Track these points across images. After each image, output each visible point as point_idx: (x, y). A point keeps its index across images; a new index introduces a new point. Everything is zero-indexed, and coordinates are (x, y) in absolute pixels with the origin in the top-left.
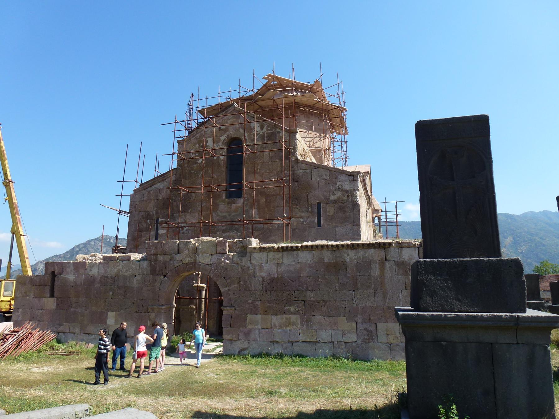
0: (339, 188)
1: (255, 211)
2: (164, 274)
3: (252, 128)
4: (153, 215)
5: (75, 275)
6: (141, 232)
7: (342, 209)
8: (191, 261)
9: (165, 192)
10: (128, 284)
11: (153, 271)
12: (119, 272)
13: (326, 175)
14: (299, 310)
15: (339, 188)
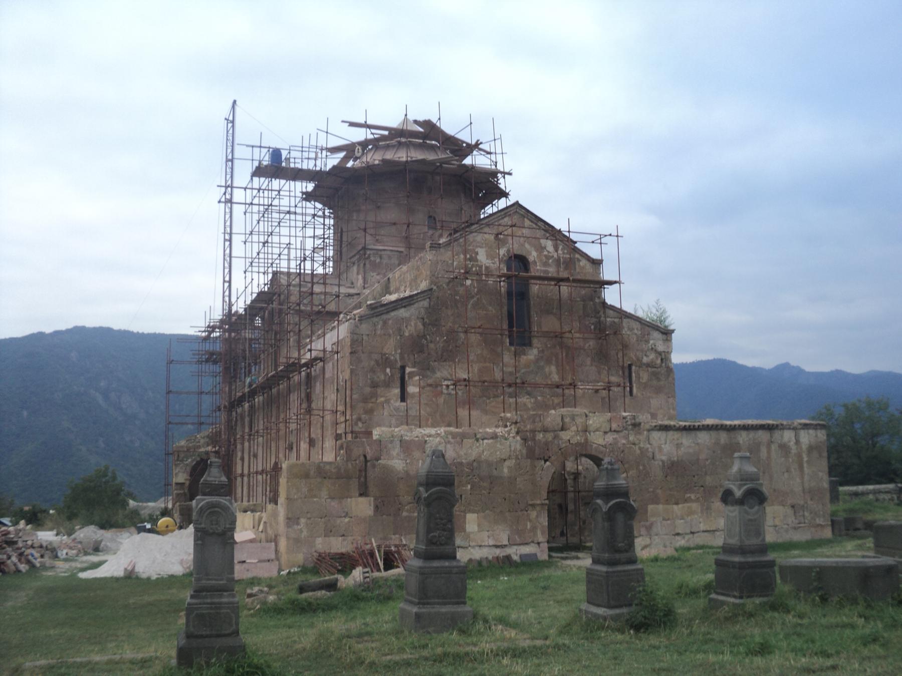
0: (652, 348)
1: (553, 368)
2: (546, 458)
3: (543, 246)
4: (396, 361)
5: (404, 462)
6: (377, 387)
7: (656, 375)
8: (581, 440)
9: (413, 325)
10: (495, 473)
11: (531, 454)
12: (480, 456)
13: (637, 329)
14: (698, 498)
15: (652, 348)
